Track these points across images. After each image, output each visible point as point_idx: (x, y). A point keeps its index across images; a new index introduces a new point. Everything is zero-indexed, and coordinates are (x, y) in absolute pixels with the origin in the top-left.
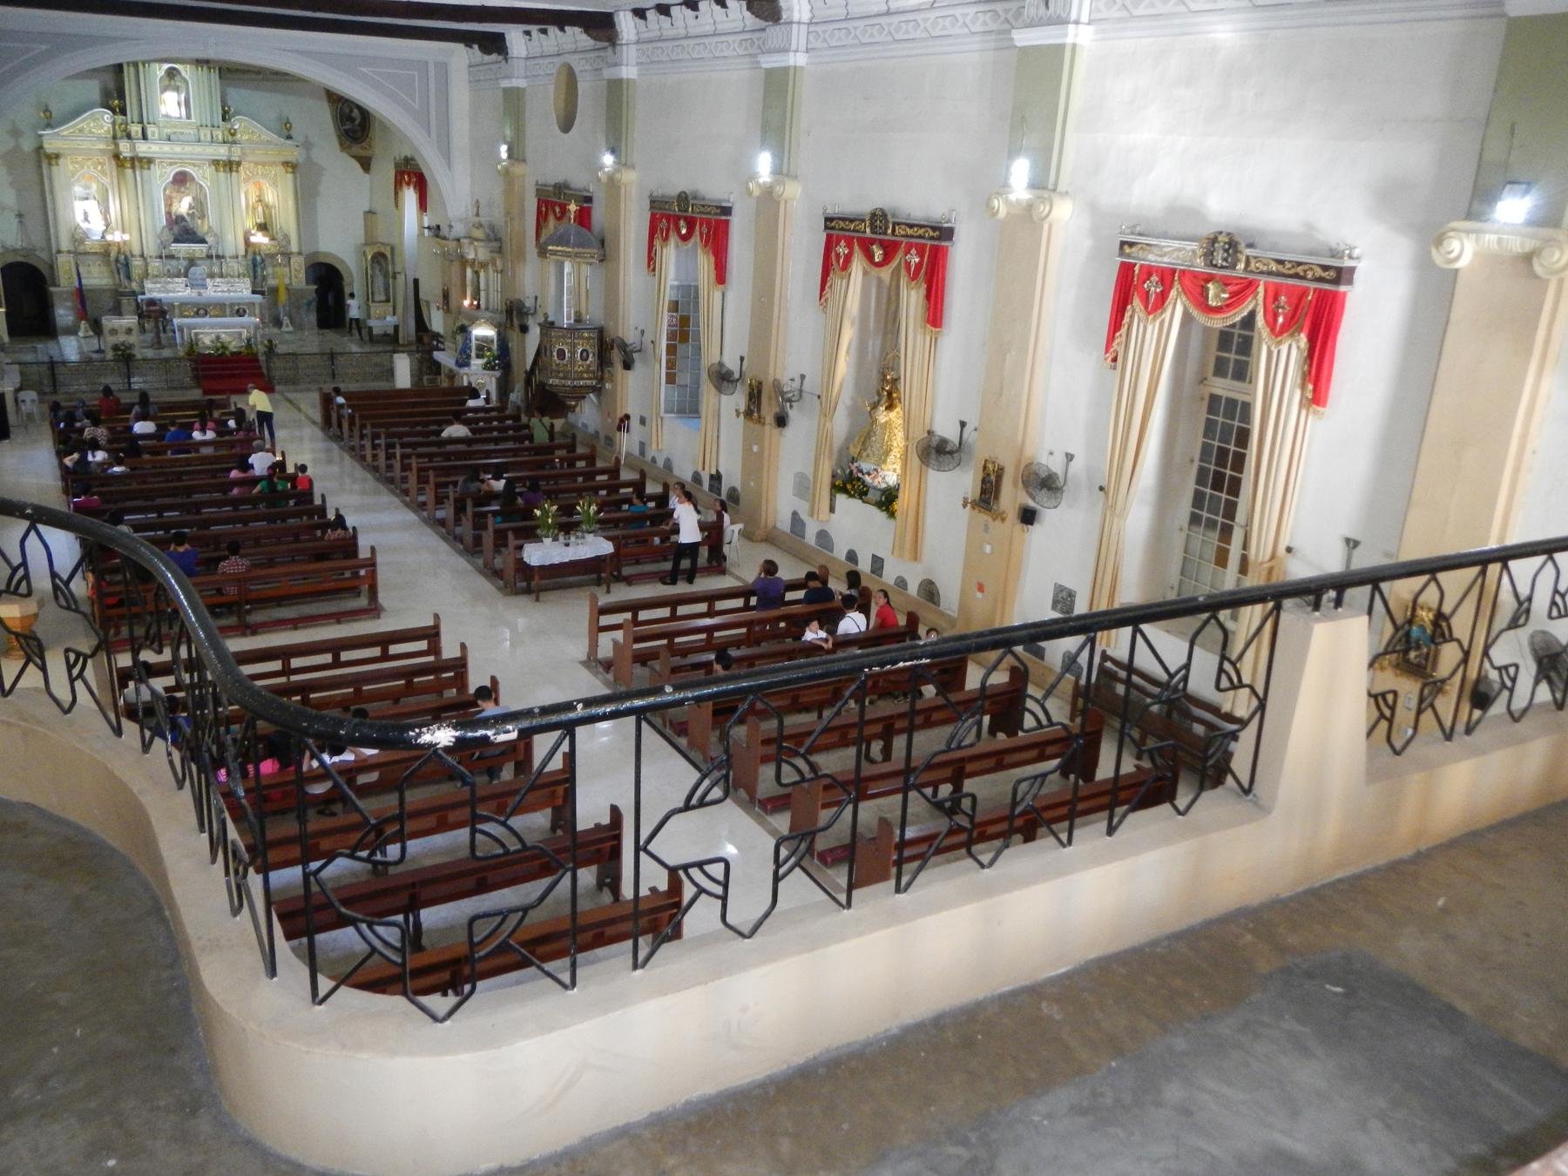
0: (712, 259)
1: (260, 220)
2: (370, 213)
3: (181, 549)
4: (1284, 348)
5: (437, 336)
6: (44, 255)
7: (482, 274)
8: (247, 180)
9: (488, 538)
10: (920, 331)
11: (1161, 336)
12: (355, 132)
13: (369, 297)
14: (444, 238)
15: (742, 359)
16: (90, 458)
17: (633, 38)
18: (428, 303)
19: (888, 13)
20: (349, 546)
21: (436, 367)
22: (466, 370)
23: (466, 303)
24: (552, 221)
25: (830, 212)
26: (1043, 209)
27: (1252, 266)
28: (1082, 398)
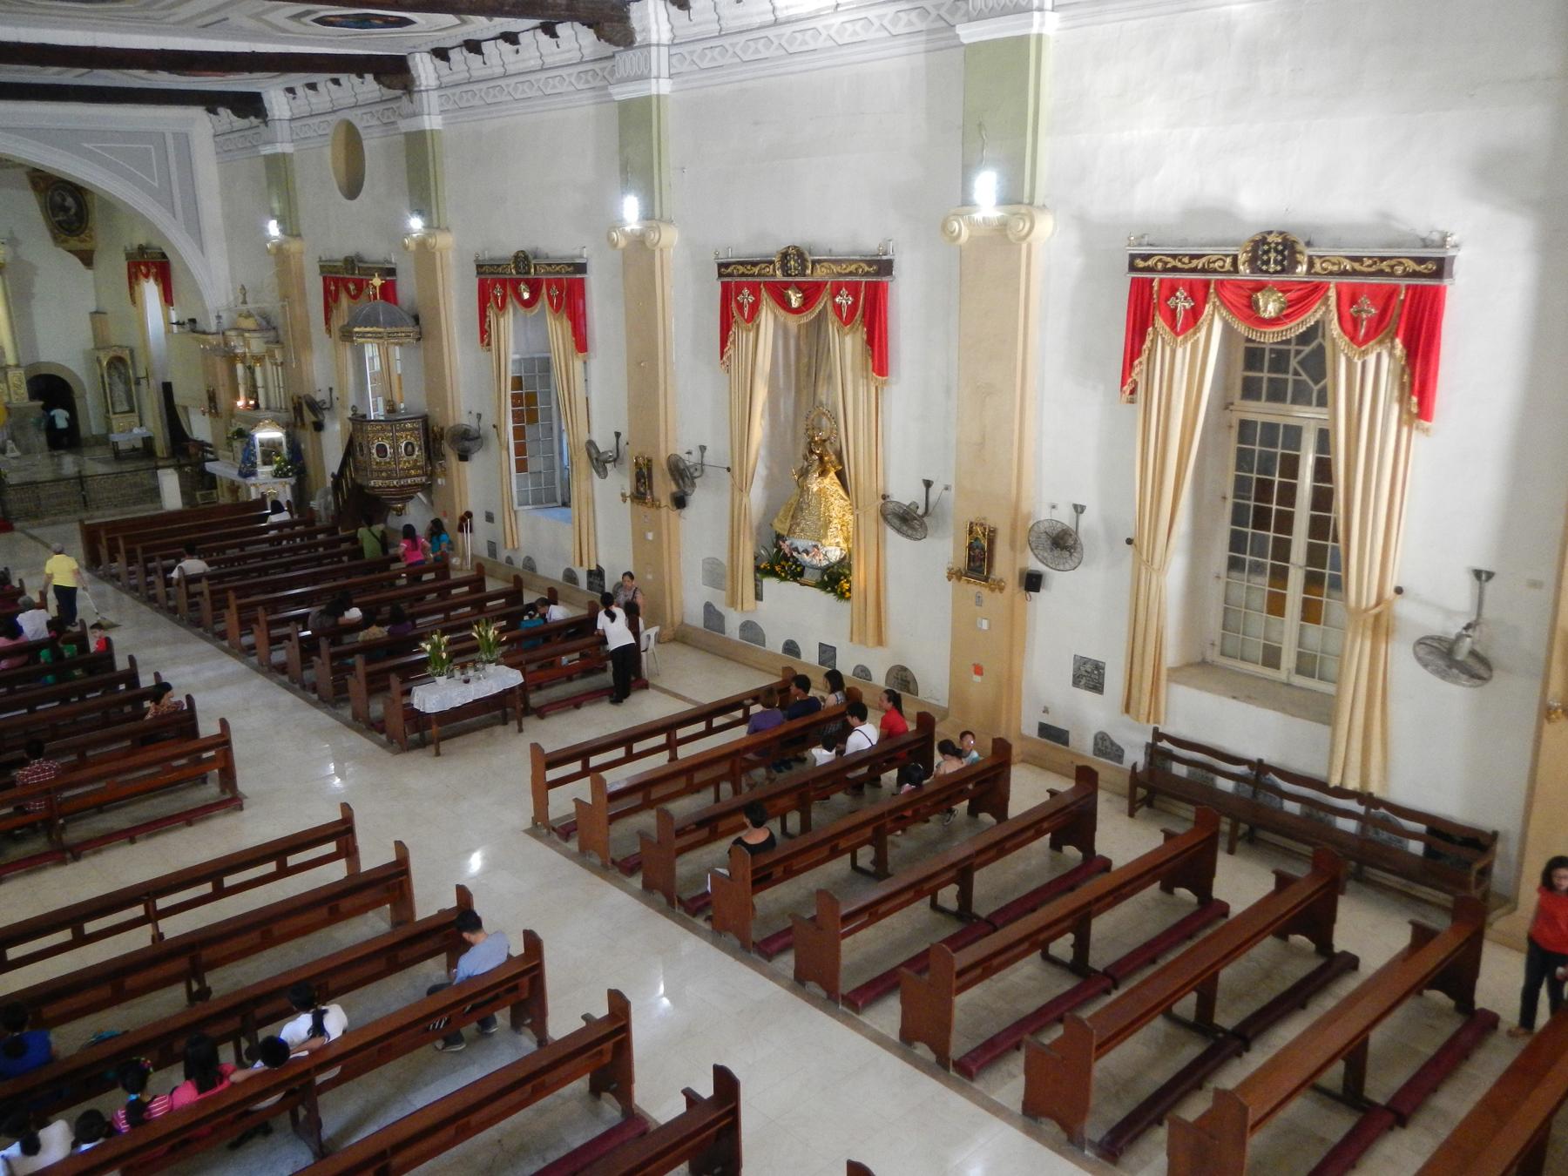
0: (567, 325)
2: (97, 314)
4: (1371, 359)
5: (202, 445)
7: (258, 370)
9: (357, 684)
11: (1195, 362)
13: (108, 410)
14: (204, 333)
15: (618, 435)
17: (433, 83)
18: (185, 408)
19: (776, 23)
20: (185, 720)
21: (211, 481)
22: (253, 480)
23: (240, 403)
24: (344, 300)
26: (1023, 227)
27: (1318, 267)
28: (1090, 436)
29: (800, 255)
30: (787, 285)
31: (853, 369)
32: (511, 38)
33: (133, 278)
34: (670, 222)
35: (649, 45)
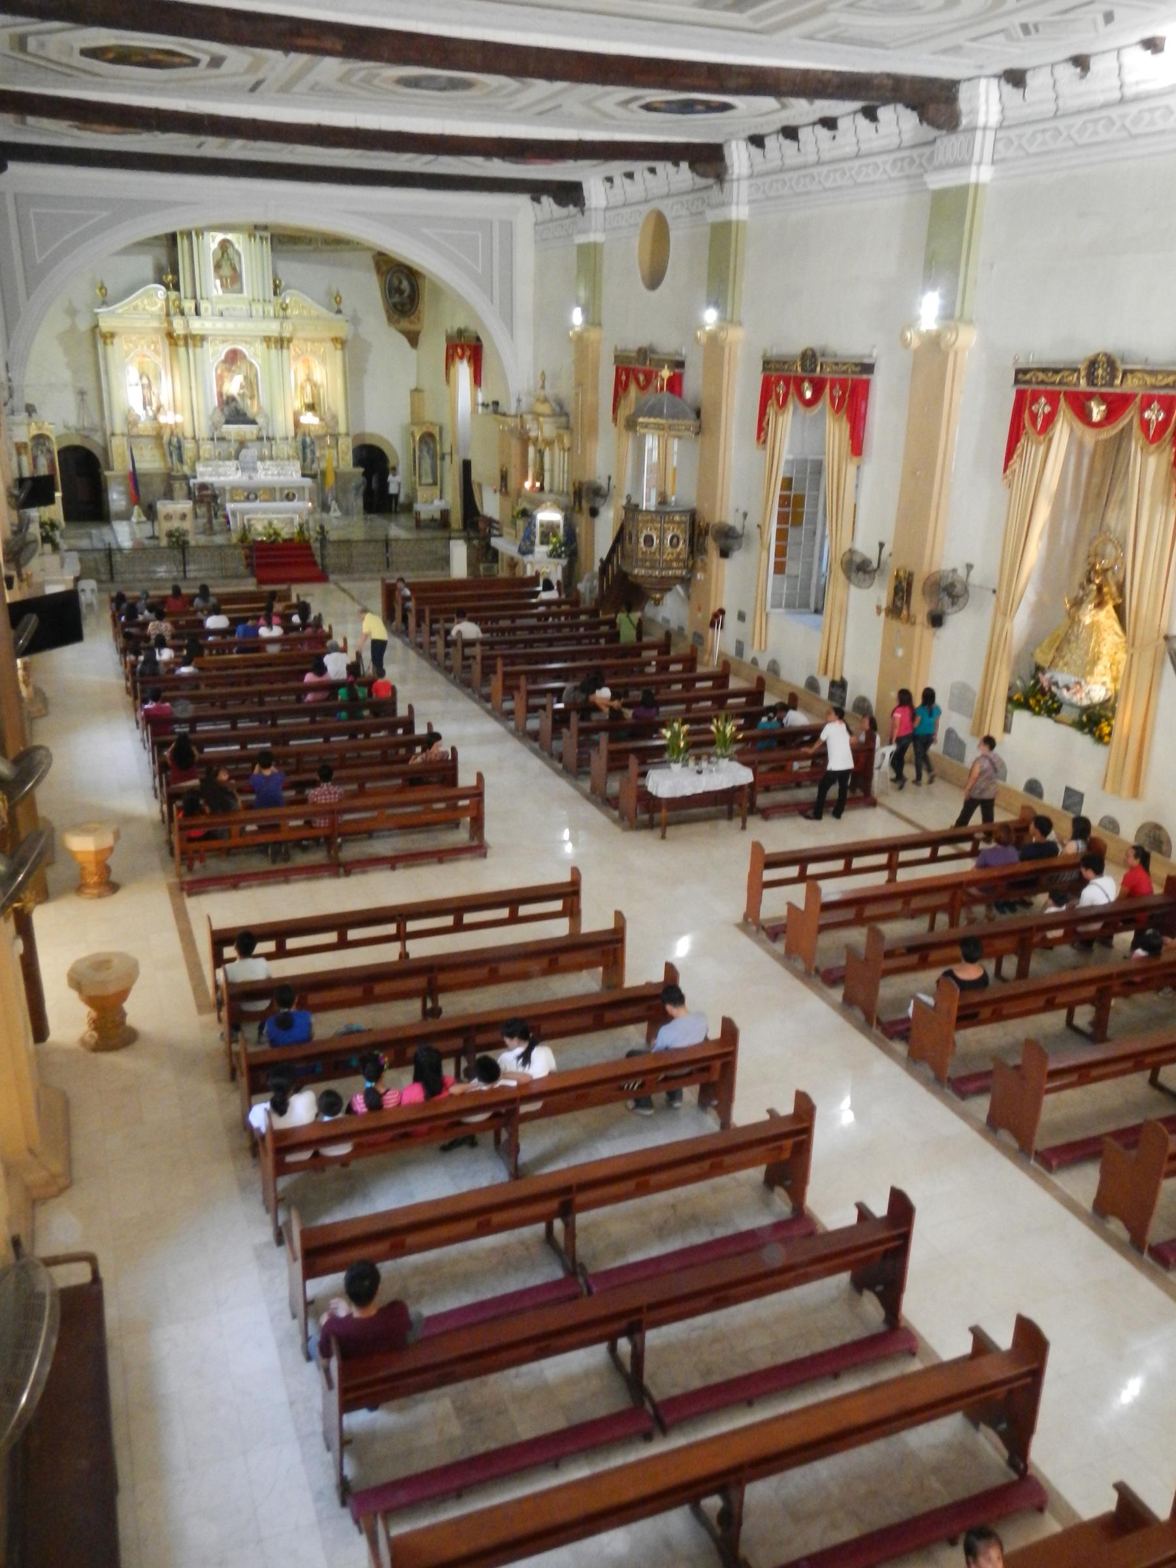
0: (846, 427)
1: (309, 400)
2: (416, 391)
3: (267, 772)
5: (490, 522)
8: (297, 357)
9: (599, 760)
12: (403, 305)
14: (504, 415)
15: (881, 545)
16: (158, 657)
17: (745, 171)
18: (480, 486)
20: (447, 769)
21: (494, 555)
22: (529, 558)
24: (633, 390)
29: (1111, 363)
30: (1090, 396)
31: (1153, 493)
32: (829, 123)
33: (450, 359)
34: (970, 322)
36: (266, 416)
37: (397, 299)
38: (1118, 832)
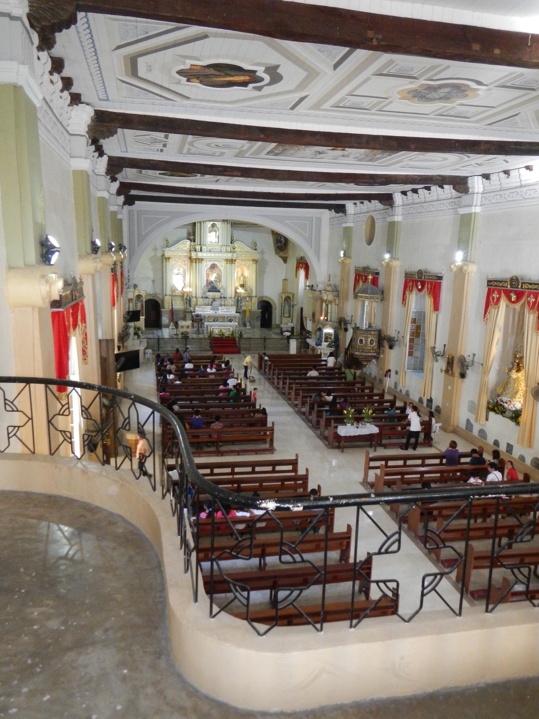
0: (432, 300)
1: (242, 283)
3: (197, 417)
5: (309, 332)
6: (161, 297)
7: (329, 306)
8: (238, 267)
10: (535, 334)
12: (281, 247)
13: (282, 315)
14: (315, 291)
15: (445, 345)
16: (168, 377)
17: (401, 203)
18: (306, 318)
19: (521, 186)
21: (307, 345)
23: (322, 318)
24: (361, 282)
25: (491, 278)
29: (517, 279)
30: (511, 291)
31: (532, 329)
33: (297, 268)
34: (474, 262)
35: (474, 193)
36: (224, 289)
37: (279, 245)
38: (525, 462)
